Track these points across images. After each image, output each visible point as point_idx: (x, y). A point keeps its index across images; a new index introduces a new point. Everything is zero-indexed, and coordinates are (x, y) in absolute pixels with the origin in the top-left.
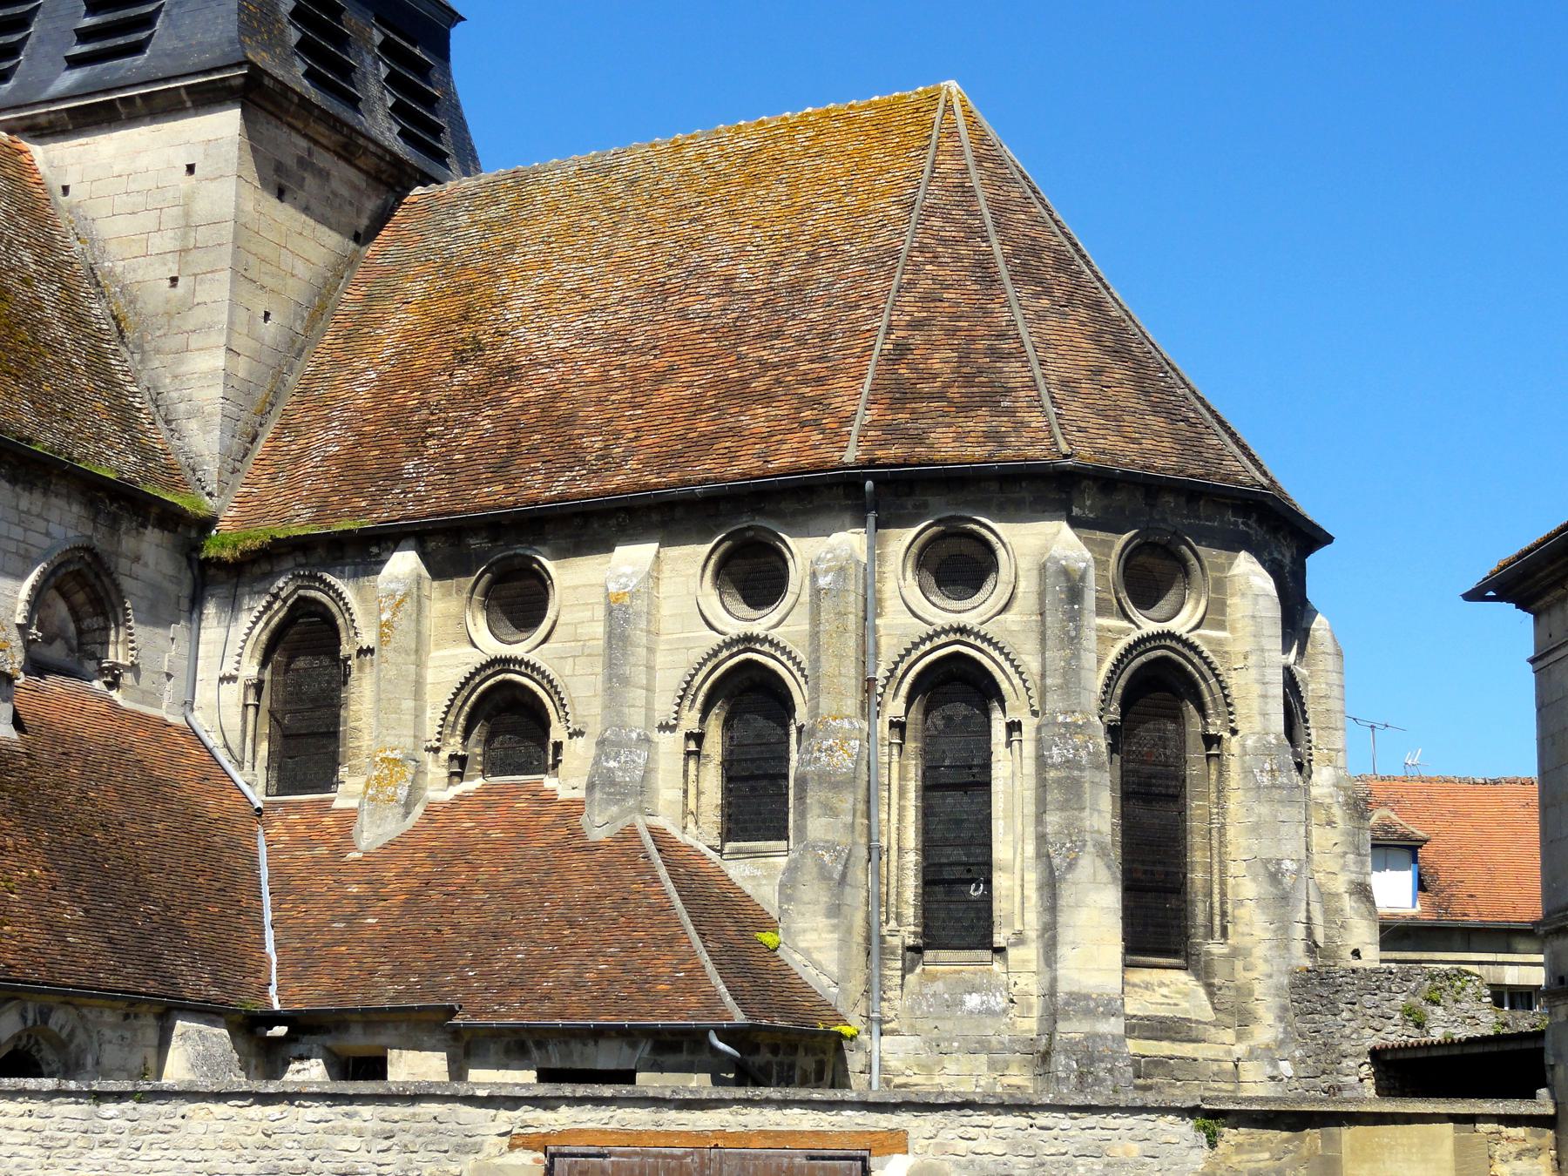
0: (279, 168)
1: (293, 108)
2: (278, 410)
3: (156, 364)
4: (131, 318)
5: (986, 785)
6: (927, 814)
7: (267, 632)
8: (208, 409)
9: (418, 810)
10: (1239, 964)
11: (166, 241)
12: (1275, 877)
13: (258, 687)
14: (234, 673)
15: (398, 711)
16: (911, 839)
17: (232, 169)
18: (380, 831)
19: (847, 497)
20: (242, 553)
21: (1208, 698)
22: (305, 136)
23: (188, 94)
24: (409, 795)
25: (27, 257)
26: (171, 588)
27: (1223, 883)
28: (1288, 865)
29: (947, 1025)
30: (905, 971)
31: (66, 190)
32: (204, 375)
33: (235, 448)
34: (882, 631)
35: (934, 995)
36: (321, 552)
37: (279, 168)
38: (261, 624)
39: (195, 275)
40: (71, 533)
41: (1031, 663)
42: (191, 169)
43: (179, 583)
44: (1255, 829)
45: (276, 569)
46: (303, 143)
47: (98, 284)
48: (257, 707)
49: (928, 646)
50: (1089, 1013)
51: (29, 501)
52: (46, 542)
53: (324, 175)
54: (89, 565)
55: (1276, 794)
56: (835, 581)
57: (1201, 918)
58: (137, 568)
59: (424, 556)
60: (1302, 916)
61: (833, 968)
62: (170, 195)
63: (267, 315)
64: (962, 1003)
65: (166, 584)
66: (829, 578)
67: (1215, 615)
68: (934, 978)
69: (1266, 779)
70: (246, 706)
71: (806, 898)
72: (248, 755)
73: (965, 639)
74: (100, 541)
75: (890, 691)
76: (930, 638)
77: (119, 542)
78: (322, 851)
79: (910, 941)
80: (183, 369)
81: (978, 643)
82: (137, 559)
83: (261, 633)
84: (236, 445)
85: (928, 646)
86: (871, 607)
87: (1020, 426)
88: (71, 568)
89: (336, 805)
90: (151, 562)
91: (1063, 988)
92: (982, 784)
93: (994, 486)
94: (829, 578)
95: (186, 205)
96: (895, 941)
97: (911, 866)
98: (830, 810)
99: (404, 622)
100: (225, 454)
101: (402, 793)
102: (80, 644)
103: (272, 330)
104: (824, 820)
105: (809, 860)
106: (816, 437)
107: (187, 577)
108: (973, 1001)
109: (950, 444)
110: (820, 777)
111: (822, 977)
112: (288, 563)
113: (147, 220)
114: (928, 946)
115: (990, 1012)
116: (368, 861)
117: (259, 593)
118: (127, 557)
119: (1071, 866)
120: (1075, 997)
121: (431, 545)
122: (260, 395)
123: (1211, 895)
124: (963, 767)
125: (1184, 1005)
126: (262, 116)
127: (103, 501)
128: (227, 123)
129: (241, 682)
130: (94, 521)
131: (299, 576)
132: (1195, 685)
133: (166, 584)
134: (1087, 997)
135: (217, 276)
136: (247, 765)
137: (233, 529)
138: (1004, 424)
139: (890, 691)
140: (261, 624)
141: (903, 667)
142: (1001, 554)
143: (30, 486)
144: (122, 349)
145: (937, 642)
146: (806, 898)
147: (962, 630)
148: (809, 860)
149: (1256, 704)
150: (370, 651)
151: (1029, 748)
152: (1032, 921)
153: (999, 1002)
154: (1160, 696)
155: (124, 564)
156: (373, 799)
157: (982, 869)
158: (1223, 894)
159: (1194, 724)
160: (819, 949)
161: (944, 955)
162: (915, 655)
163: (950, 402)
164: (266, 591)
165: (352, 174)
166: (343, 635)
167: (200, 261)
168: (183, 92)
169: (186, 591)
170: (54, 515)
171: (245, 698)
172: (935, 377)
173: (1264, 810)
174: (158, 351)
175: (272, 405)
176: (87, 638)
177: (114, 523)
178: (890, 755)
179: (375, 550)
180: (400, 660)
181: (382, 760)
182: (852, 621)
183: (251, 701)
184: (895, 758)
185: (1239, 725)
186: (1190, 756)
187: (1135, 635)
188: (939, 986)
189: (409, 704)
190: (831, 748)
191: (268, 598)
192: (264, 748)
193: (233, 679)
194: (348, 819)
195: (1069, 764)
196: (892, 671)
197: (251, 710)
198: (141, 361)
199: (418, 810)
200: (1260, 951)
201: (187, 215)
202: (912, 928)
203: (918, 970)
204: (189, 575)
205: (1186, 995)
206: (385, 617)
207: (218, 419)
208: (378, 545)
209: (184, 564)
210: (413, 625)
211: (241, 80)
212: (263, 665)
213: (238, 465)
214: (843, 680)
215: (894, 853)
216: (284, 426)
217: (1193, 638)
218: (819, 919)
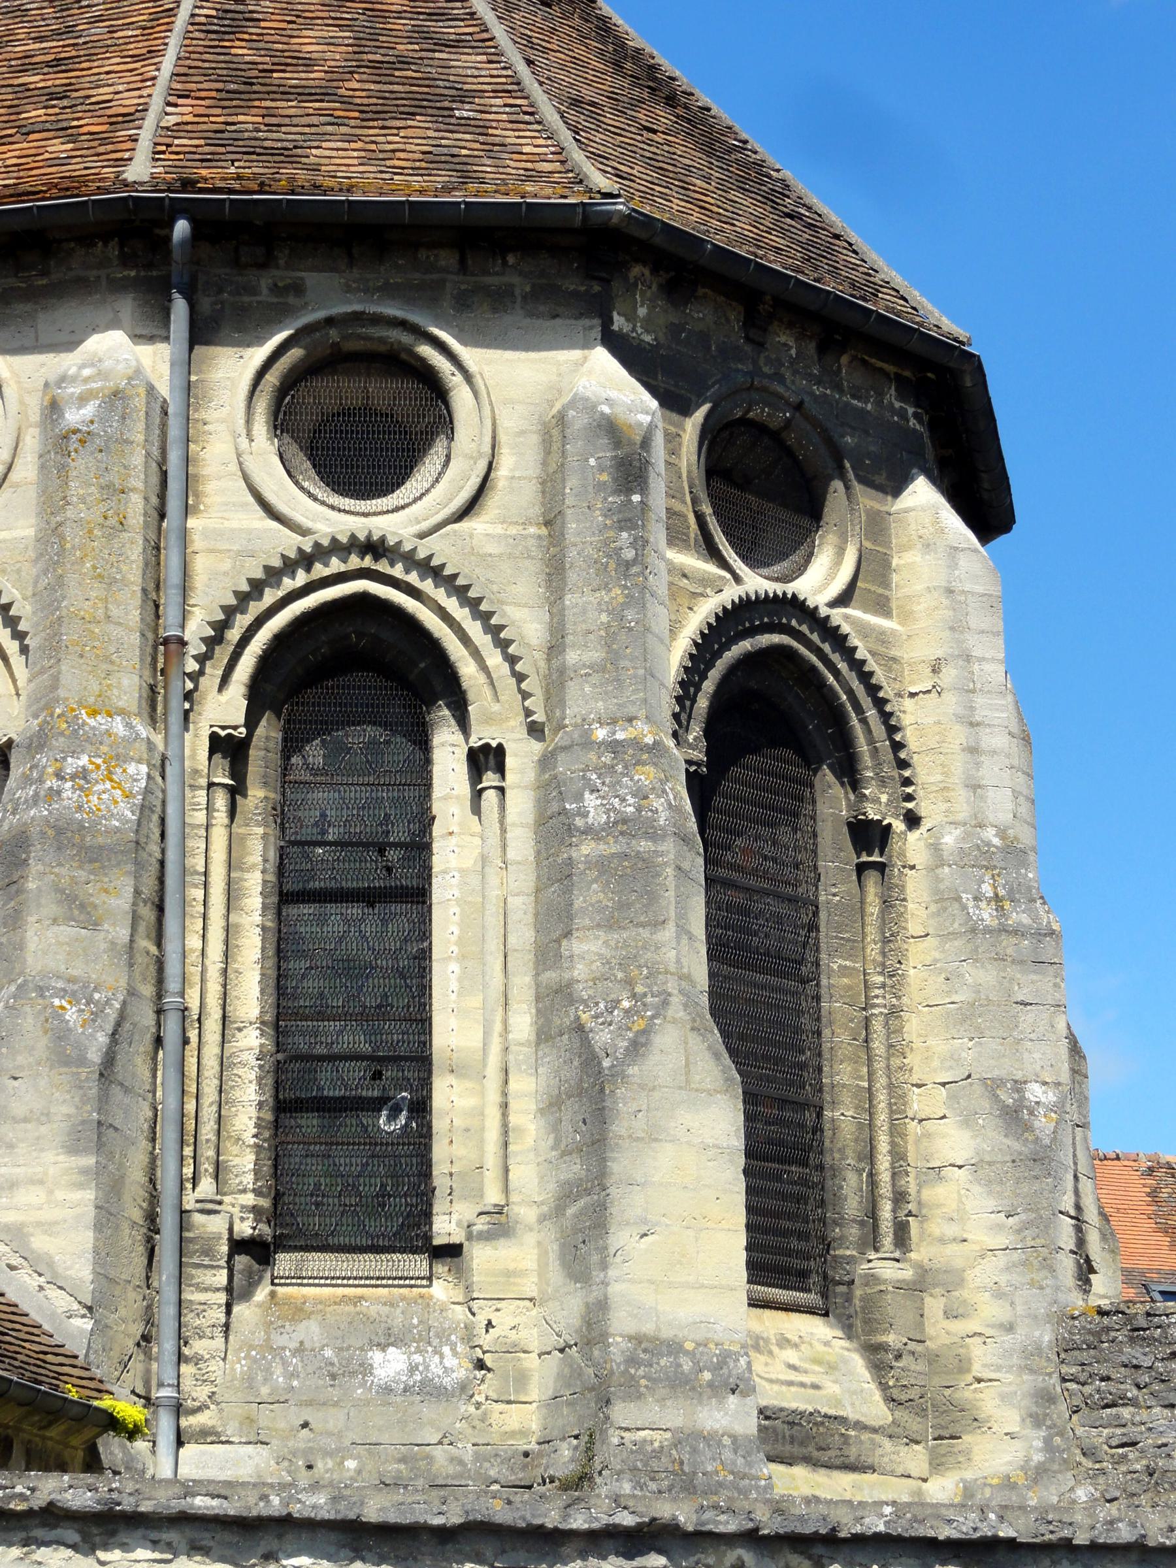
5: (418, 895)
6: (283, 947)
10: (934, 1305)
12: (1015, 1117)
16: (251, 998)
19: (126, 261)
21: (862, 746)
27: (896, 1131)
28: (1035, 1092)
29: (329, 1420)
30: (234, 1294)
34: (197, 542)
35: (300, 1350)
41: (528, 625)
44: (967, 1017)
49: (301, 578)
50: (681, 1385)
55: (1009, 945)
56: (101, 418)
57: (852, 1206)
60: (1068, 1203)
61: (81, 1271)
64: (366, 1369)
66: (89, 410)
67: (868, 583)
68: (298, 1312)
69: (987, 915)
71: (18, 1108)
73: (383, 566)
75: (214, 671)
76: (306, 560)
79: (245, 1229)
81: (413, 578)
85: (301, 578)
86: (171, 493)
87: (494, 149)
91: (622, 1324)
92: (407, 893)
93: (447, 259)
94: (89, 410)
96: (216, 1225)
97: (250, 1058)
98: (79, 910)
104: (66, 931)
105: (29, 1022)
106: (58, 147)
108: (390, 1365)
109: (349, 165)
110: (60, 831)
111: (53, 1293)
114: (282, 1244)
115: (430, 1391)
119: (638, 1047)
120: (649, 1347)
123: (870, 1156)
124: (366, 845)
125: (832, 1388)
132: (838, 719)
134: (674, 1348)
138: (465, 144)
139: (214, 671)
141: (242, 621)
142: (461, 397)
145: (320, 570)
146: (18, 1108)
147: (375, 548)
148: (29, 1022)
149: (959, 765)
151: (521, 803)
152: (532, 1182)
153: (451, 1365)
154: (777, 725)
157: (406, 1065)
158: (898, 1155)
159: (832, 803)
160: (48, 1227)
161: (318, 1262)
162: (270, 597)
163: (346, 102)
172: (309, 63)
173: (982, 976)
178: (209, 808)
182: (136, 507)
184: (221, 817)
185: (923, 807)
186: (827, 865)
187: (731, 594)
188: (310, 1331)
190: (83, 774)
195: (622, 826)
196: (221, 628)
200: (983, 1275)
202: (249, 1199)
203: (261, 1294)
205: (831, 1368)
214: (116, 632)
215: (212, 1025)
217: (837, 616)
218: (49, 1156)
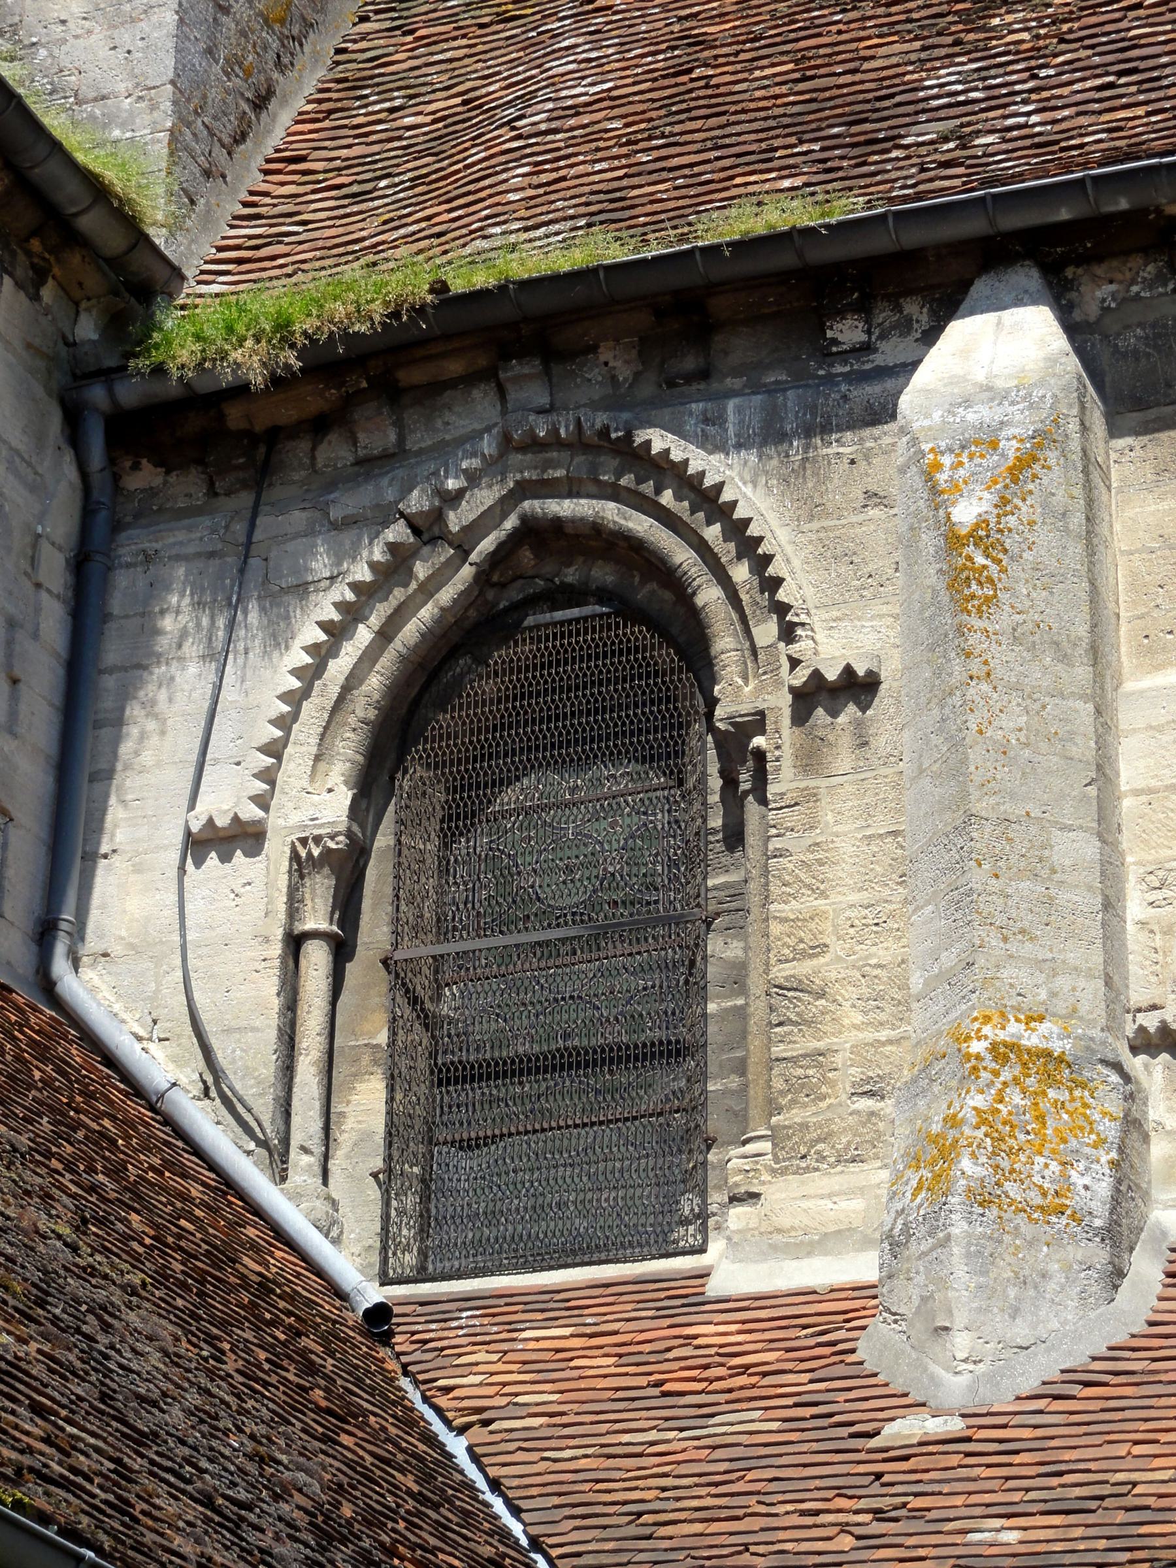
2: (323, 44)
7: (387, 662)
9: (1146, 1270)
13: (347, 867)
14: (251, 812)
15: (1040, 867)
18: (1021, 1332)
24: (1117, 1199)
36: (616, 360)
38: (364, 635)
43: (36, 488)
45: (418, 439)
48: (342, 950)
59: (1072, 329)
70: (295, 942)
72: (306, 1123)
78: (752, 1421)
83: (365, 666)
84: (221, 87)
89: (715, 1287)
99: (1044, 537)
100: (189, 97)
101: (1092, 1186)
112: (475, 416)
116: (984, 1441)
117: (350, 522)
121: (1097, 294)
129: (277, 850)
131: (533, 445)
136: (302, 1164)
137: (224, 316)
140: (364, 635)
150: (858, 687)
156: (983, 1198)
164: (385, 516)
166: (725, 645)
169: (61, 526)
171: (293, 909)
179: (847, 332)
180: (1035, 675)
181: (1002, 1052)
183: (317, 918)
189: (1076, 849)
191: (397, 532)
192: (367, 1104)
193: (243, 837)
194: (824, 1327)
197: (317, 957)
199: (1146, 1270)
204: (70, 472)
206: (965, 513)
208: (864, 309)
210: (1076, 549)
212: (372, 786)
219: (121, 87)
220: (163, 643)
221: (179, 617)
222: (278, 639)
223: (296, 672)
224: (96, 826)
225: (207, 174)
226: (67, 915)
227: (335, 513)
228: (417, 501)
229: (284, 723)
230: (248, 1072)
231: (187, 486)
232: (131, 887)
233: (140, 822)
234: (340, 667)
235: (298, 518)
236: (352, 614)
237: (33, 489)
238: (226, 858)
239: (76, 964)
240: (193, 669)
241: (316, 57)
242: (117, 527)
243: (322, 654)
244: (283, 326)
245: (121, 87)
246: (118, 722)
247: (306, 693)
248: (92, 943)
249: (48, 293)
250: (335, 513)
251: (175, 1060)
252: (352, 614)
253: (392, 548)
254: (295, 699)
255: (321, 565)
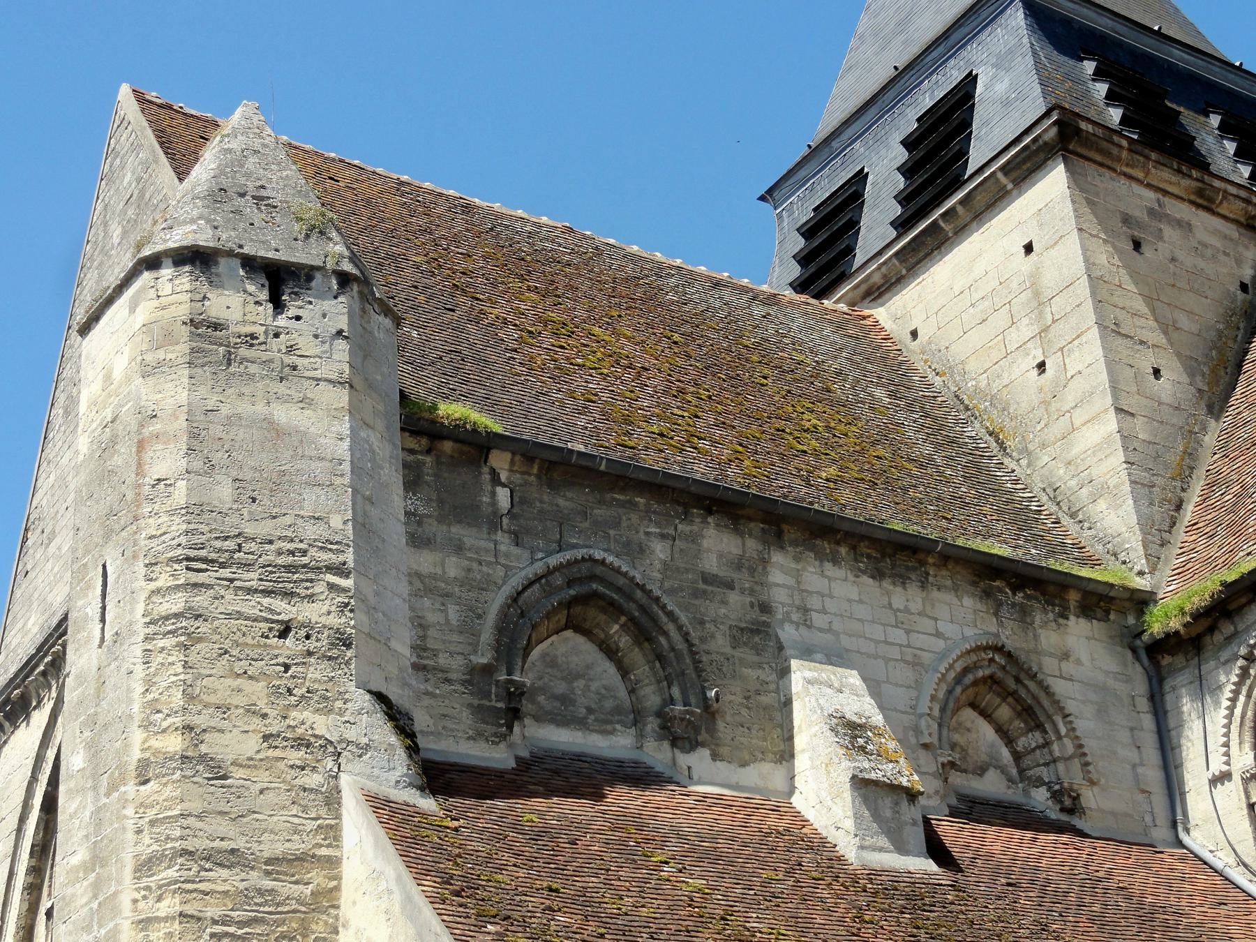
0: (1127, 220)
1: (1125, 154)
2: (1201, 472)
3: (1046, 459)
4: (1007, 423)
8: (1112, 483)
11: (1026, 330)
17: (1072, 223)
20: (1192, 615)
22: (1149, 186)
23: (1006, 174)
25: (879, 393)
26: (1122, 688)
31: (914, 334)
32: (1098, 447)
33: (1157, 517)
37: (1127, 220)
38: (1242, 698)
39: (1061, 349)
40: (969, 632)
42: (1029, 248)
43: (1128, 680)
45: (1241, 627)
46: (1150, 194)
47: (967, 409)
51: (906, 597)
52: (941, 645)
53: (1181, 224)
54: (1004, 668)
58: (1067, 667)
62: (1014, 285)
63: (1157, 372)
65: (1110, 682)
74: (1010, 636)
77: (1036, 637)
80: (1075, 451)
82: (1066, 656)
84: (1159, 513)
88: (980, 673)
90: (1085, 658)
95: (1034, 286)
100: (1146, 525)
102: (1021, 772)
103: (1168, 386)
107: (1137, 674)
113: (1001, 320)
117: (1227, 662)
118: (1051, 655)
122: (1173, 458)
126: (1091, 169)
127: (1000, 590)
128: (1054, 183)
129: (1236, 777)
130: (996, 614)
133: (1110, 682)
135: (1084, 338)
140: (1242, 698)
143: (902, 579)
144: (1006, 461)
155: (1049, 665)
164: (1236, 657)
165: (1217, 222)
167: (1063, 332)
168: (1000, 175)
170: (942, 611)
174: (1043, 446)
175: (1192, 468)
176: (1027, 761)
177: (1023, 614)
191: (1241, 662)
193: (1225, 777)
198: (1029, 465)
201: (1037, 294)
204: (1139, 669)
207: (1127, 487)
209: (1129, 654)
211: (1054, 131)
213: (1166, 536)
216: (1210, 485)
219: (1124, 529)
220: (1186, 717)
221: (1187, 705)
222: (1217, 704)
223: (1225, 717)
224: (1181, 783)
225: (1162, 545)
226: (1179, 817)
227: (1222, 660)
228: (1243, 651)
229: (1227, 735)
230: (1248, 855)
231: (1179, 660)
232: (1197, 801)
233: (1195, 776)
234: (1238, 711)
235: (1212, 663)
236: (1236, 693)
237: (1127, 682)
238: (1223, 784)
239: (1187, 831)
240: (1197, 722)
241: (1198, 479)
242: (1161, 681)
243: (1231, 709)
244: (1182, 611)
245: (1124, 529)
246: (1180, 746)
247: (1230, 723)
248: (1192, 822)
249: (1112, 617)
250: (1222, 660)
251: (1227, 856)
252: (1236, 693)
253: (1241, 668)
254: (1228, 726)
255: (1223, 678)
